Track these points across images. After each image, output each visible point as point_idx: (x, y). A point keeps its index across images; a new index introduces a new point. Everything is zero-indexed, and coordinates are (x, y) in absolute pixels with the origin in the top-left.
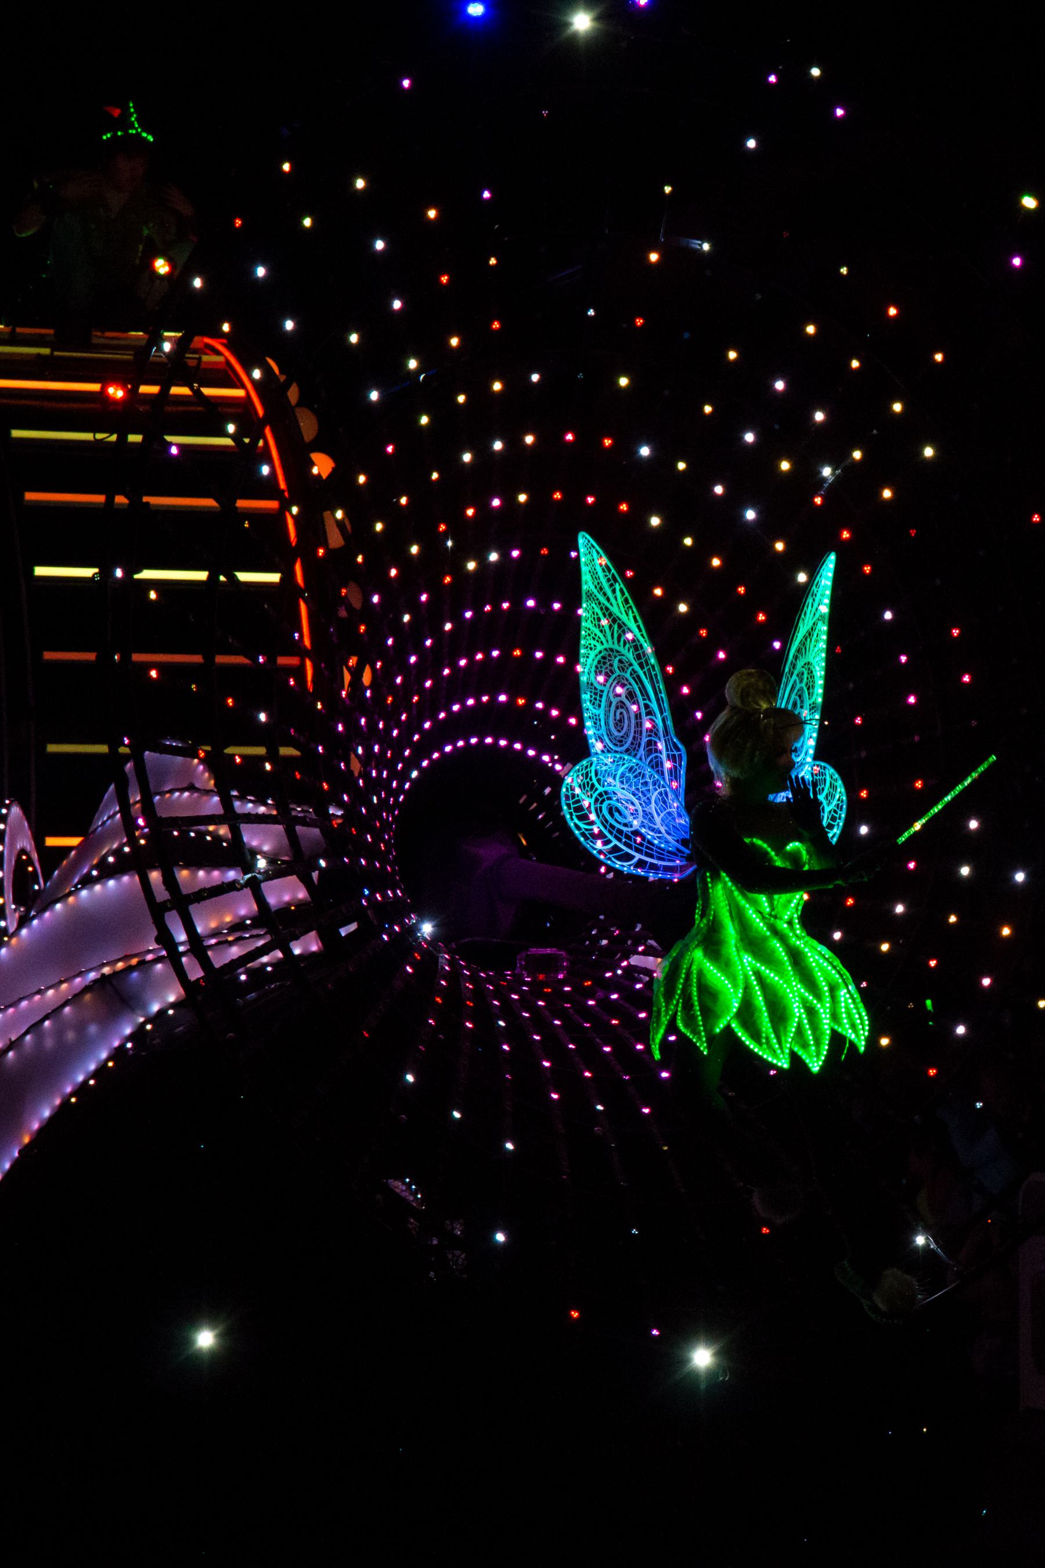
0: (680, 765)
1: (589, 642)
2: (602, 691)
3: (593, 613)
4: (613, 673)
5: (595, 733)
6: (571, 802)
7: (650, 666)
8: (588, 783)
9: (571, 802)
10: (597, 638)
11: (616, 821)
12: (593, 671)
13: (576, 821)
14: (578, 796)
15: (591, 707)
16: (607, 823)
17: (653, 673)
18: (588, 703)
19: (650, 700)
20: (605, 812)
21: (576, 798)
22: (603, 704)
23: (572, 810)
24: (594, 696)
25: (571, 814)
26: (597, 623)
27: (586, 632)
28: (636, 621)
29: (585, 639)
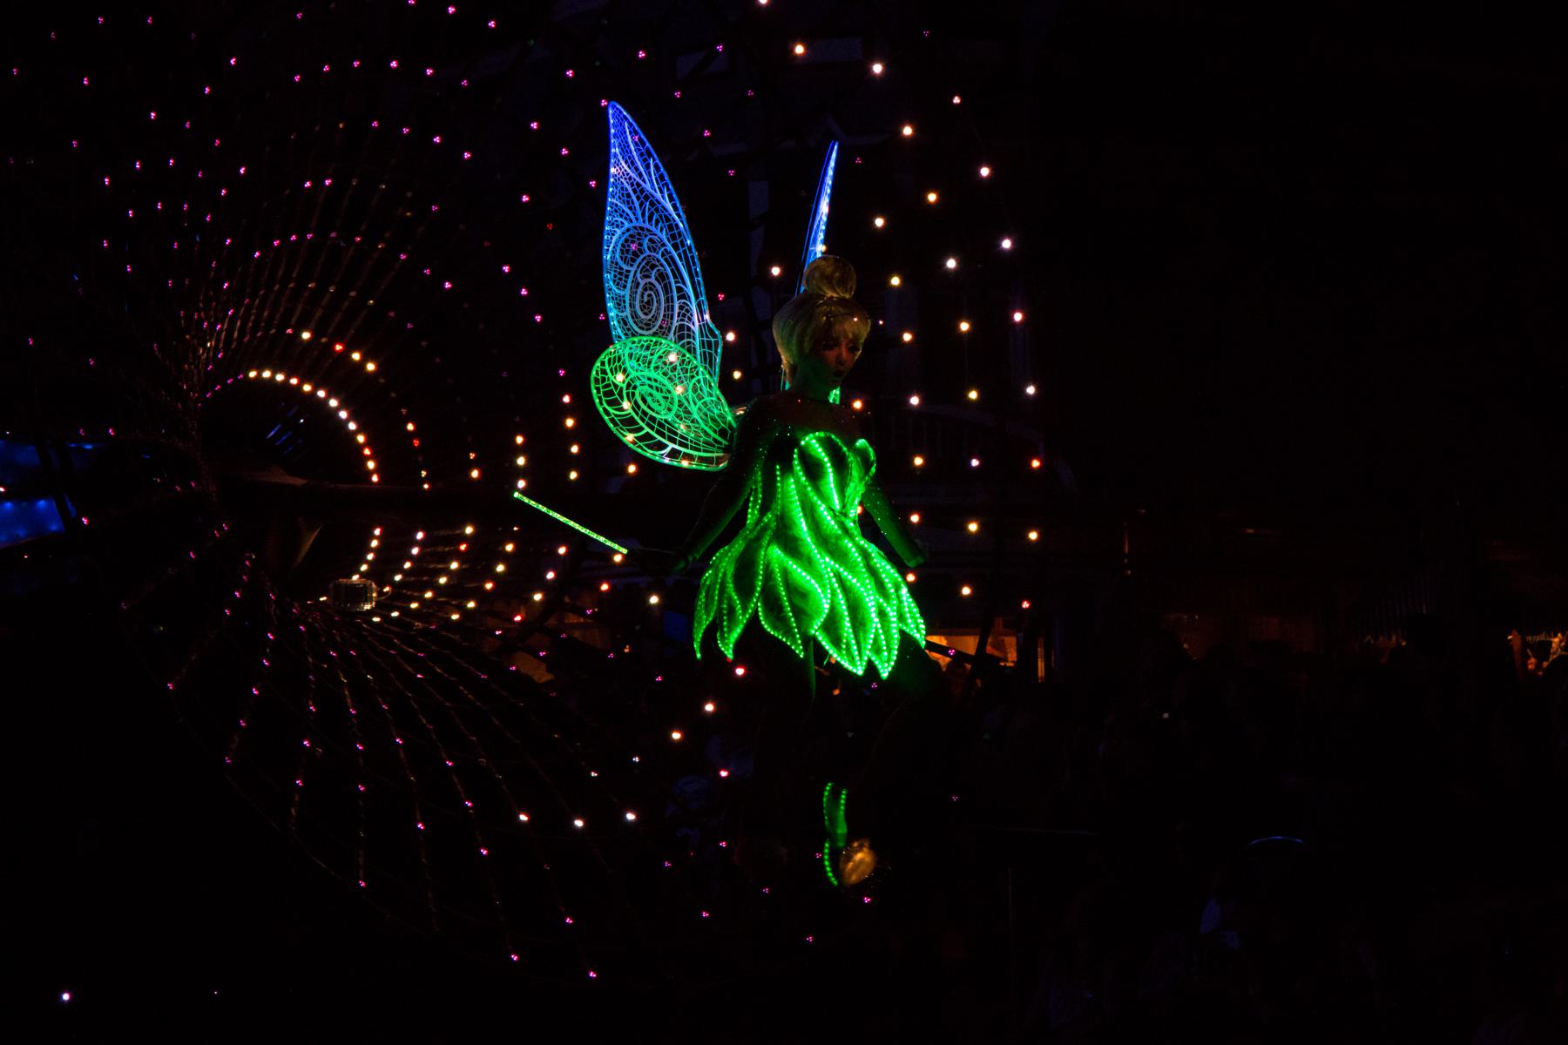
0: (716, 352)
1: (616, 219)
2: (628, 271)
3: (622, 188)
4: (642, 253)
5: (617, 315)
6: (601, 386)
7: (686, 248)
8: (620, 367)
9: (601, 386)
10: (625, 215)
11: (649, 407)
12: (618, 250)
13: (605, 405)
14: (609, 380)
15: (614, 288)
16: (639, 409)
17: (689, 255)
18: (611, 283)
19: (684, 284)
20: (638, 397)
21: (607, 382)
22: (629, 285)
23: (602, 395)
24: (618, 276)
25: (600, 398)
26: (626, 199)
27: (612, 208)
28: (671, 199)
29: (610, 215)
